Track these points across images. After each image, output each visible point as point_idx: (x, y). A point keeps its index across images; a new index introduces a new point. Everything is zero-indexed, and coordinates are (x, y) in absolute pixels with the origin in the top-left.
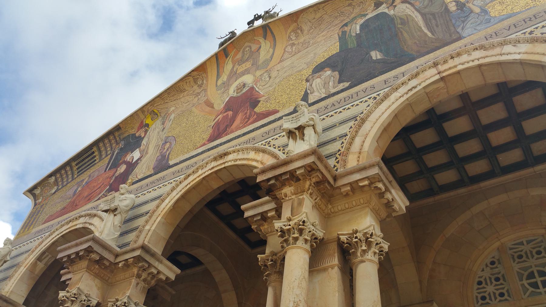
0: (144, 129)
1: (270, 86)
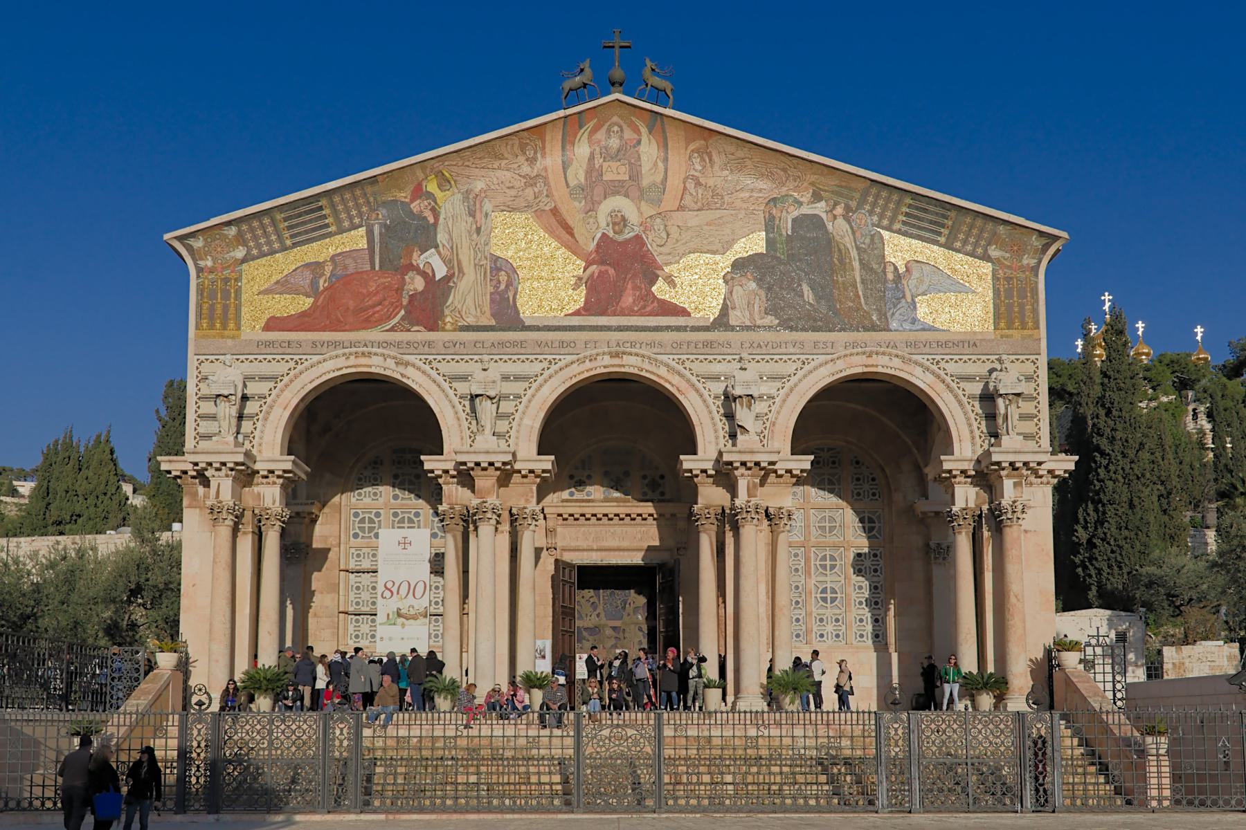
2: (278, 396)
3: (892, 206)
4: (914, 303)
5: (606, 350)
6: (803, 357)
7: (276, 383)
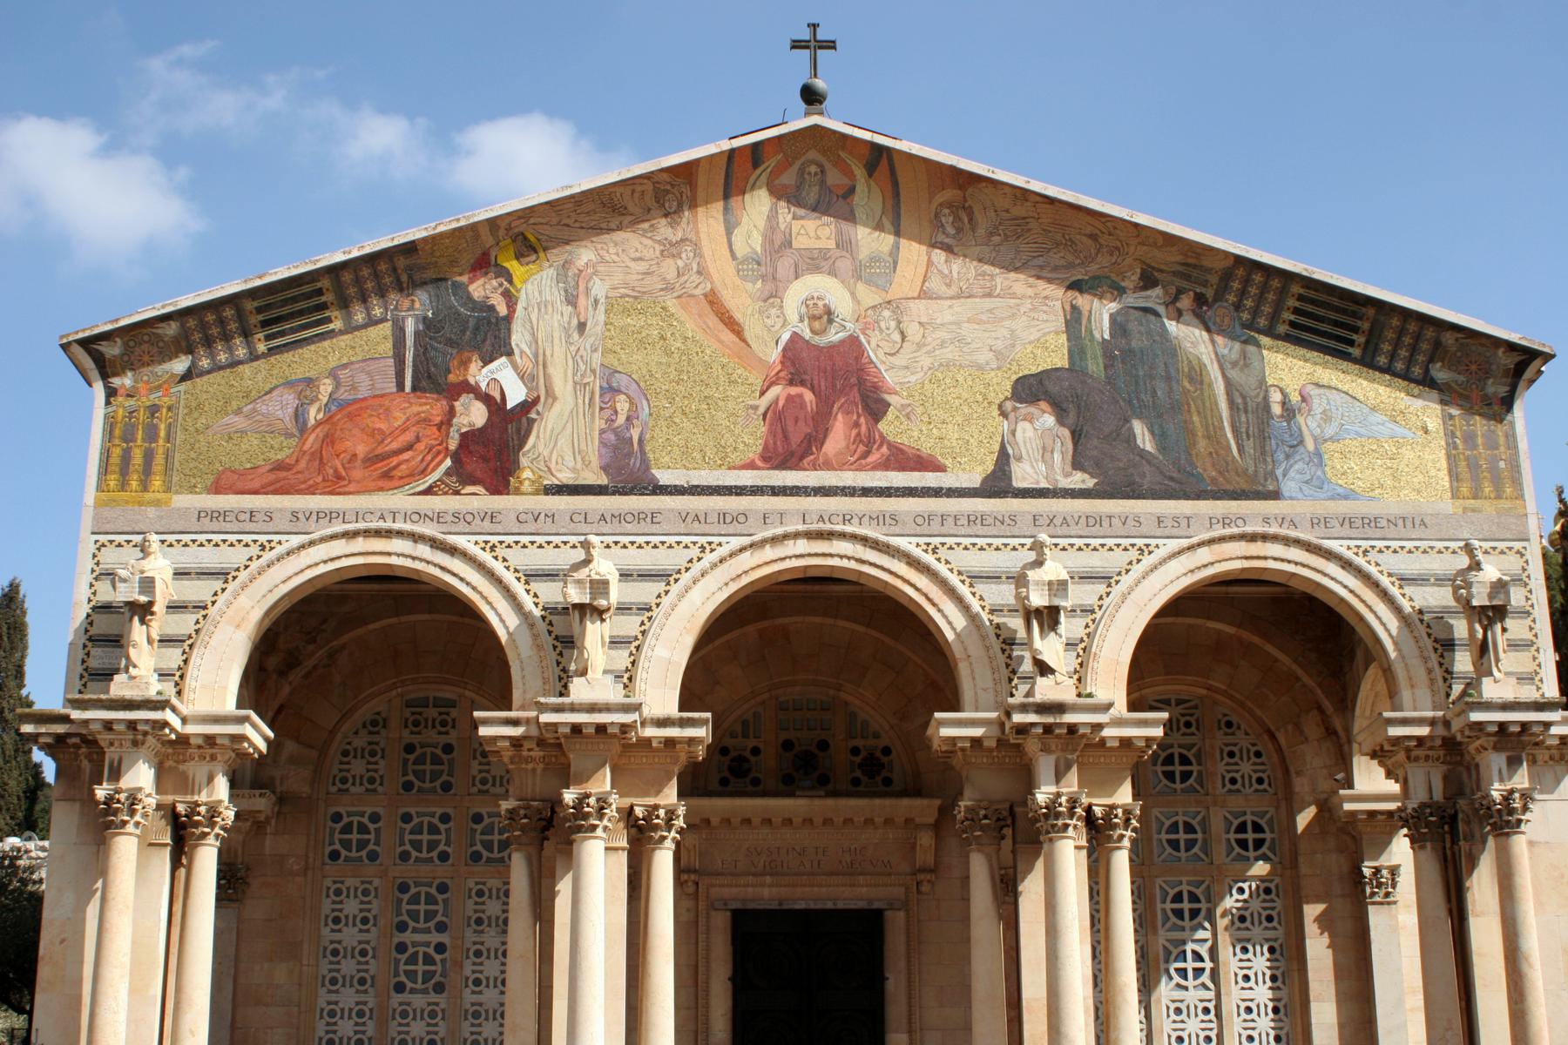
0: (495, 283)
1: (907, 368)
2: (229, 604)
3: (1271, 296)
4: (1319, 455)
5: (801, 528)
6: (1140, 542)
7: (226, 581)
